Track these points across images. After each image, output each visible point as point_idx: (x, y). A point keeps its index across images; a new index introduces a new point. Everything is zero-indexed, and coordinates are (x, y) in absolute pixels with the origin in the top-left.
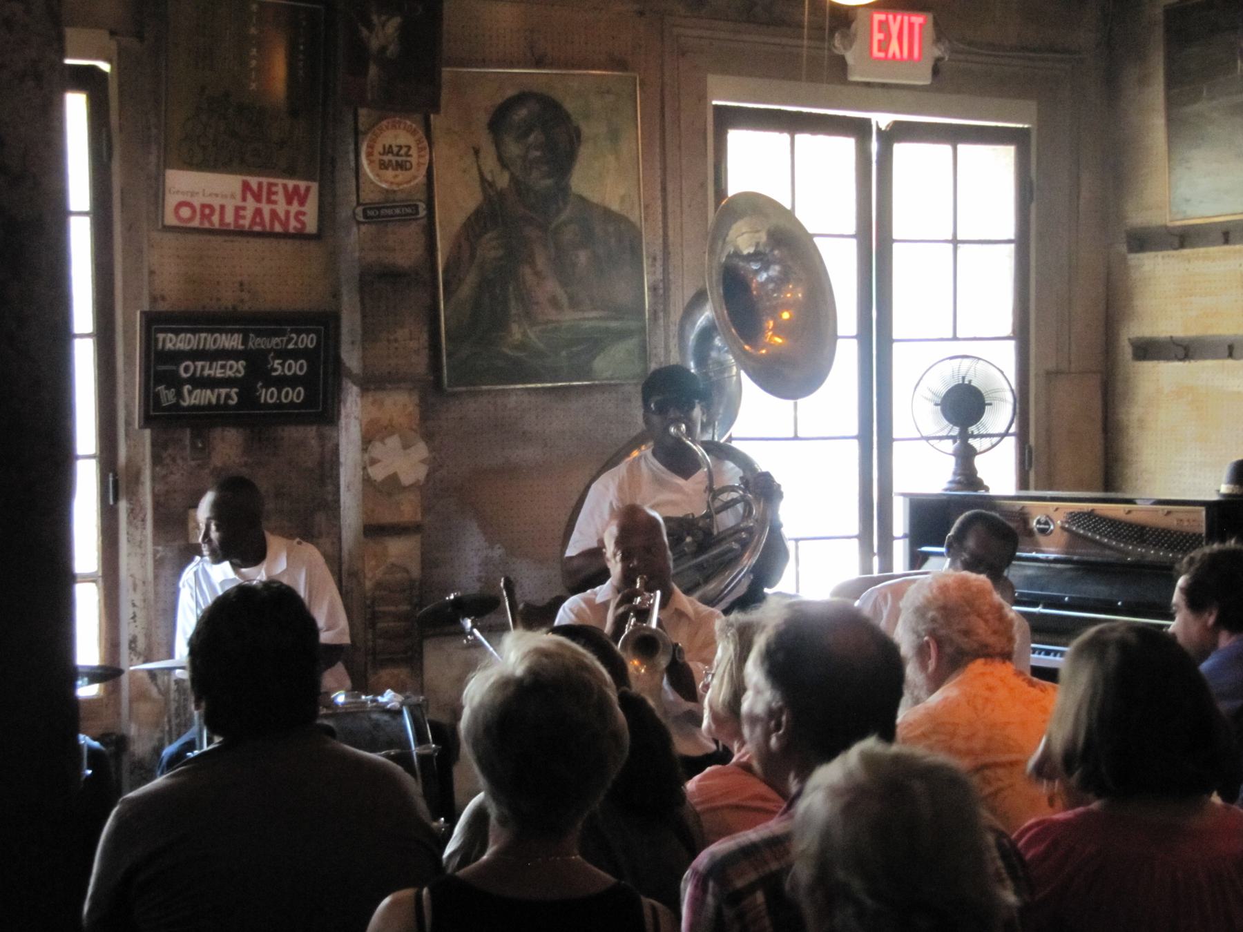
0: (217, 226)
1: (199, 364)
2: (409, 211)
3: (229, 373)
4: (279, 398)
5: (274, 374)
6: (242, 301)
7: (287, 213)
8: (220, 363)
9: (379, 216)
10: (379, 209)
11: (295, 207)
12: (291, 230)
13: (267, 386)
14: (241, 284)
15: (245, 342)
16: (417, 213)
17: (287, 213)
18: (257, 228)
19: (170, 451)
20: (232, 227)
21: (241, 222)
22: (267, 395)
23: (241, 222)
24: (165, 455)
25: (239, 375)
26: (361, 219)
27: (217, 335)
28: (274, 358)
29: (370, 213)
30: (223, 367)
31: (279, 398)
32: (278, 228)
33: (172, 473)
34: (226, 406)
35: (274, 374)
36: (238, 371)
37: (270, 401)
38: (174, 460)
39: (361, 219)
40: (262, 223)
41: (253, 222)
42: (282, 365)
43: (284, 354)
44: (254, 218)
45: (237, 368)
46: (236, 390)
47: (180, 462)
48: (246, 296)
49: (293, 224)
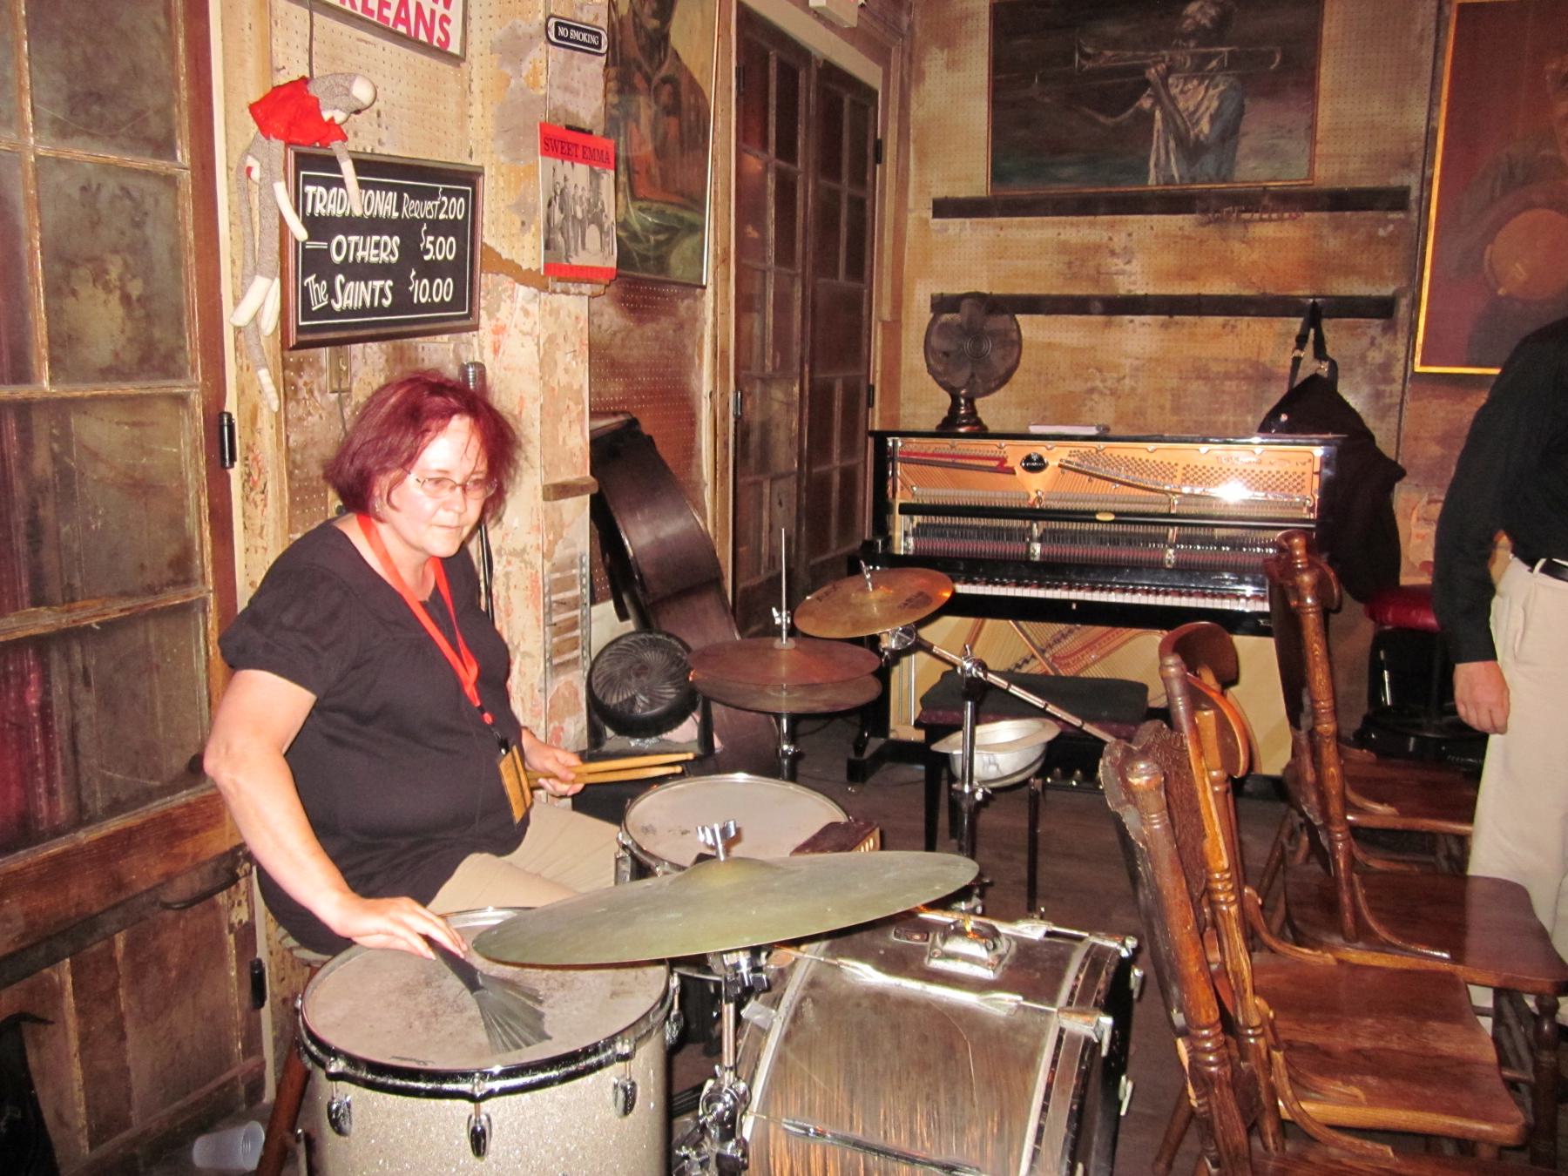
0: (359, 12)
1: (353, 239)
2: (594, 40)
3: (384, 256)
4: (431, 296)
5: (427, 258)
6: (380, 142)
7: (433, 12)
8: (375, 238)
9: (568, 39)
10: (570, 27)
11: (440, 9)
12: (436, 44)
13: (419, 277)
14: (379, 115)
15: (399, 208)
16: (599, 47)
17: (433, 12)
18: (402, 29)
19: (306, 378)
20: (375, 19)
21: (386, 12)
22: (420, 290)
23: (386, 12)
24: (300, 383)
25: (394, 260)
26: (553, 38)
27: (371, 192)
28: (427, 233)
29: (562, 31)
30: (377, 246)
31: (431, 296)
32: (423, 37)
33: (309, 414)
34: (381, 310)
35: (427, 258)
36: (392, 253)
37: (423, 300)
38: (311, 392)
39: (553, 38)
40: (406, 22)
41: (398, 19)
42: (433, 243)
43: (437, 228)
44: (398, 12)
45: (385, 250)
46: (390, 283)
47: (316, 393)
48: (384, 136)
49: (438, 33)
